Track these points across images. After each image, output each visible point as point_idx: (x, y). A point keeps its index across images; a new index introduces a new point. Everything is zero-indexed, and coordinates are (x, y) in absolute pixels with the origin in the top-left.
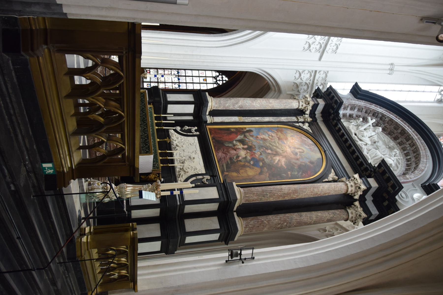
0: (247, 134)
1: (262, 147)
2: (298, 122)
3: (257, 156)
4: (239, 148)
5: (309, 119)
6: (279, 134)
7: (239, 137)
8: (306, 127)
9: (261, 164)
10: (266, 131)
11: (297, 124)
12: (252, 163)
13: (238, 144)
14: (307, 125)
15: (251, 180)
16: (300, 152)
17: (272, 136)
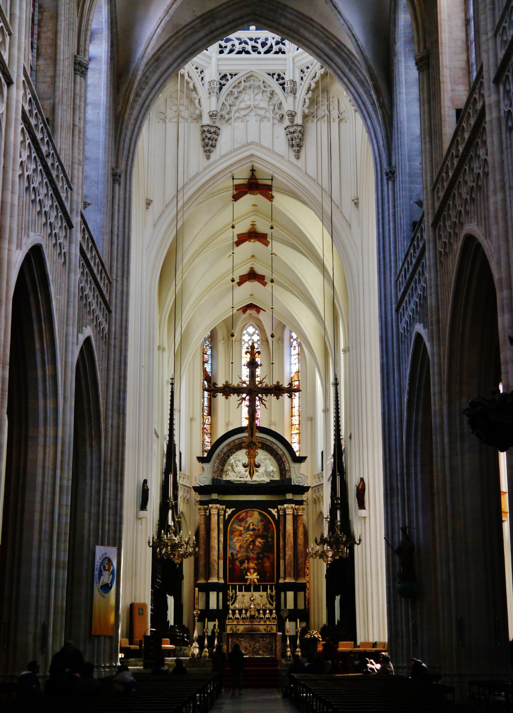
0: (235, 557)
1: (247, 551)
2: (224, 515)
3: (254, 556)
4: (248, 566)
5: (224, 507)
6: (235, 534)
7: (237, 563)
8: (229, 511)
9: (261, 556)
10: (232, 543)
11: (227, 517)
12: (260, 561)
13: (244, 566)
14: (228, 510)
15: (272, 565)
16: (253, 525)
17: (237, 540)
